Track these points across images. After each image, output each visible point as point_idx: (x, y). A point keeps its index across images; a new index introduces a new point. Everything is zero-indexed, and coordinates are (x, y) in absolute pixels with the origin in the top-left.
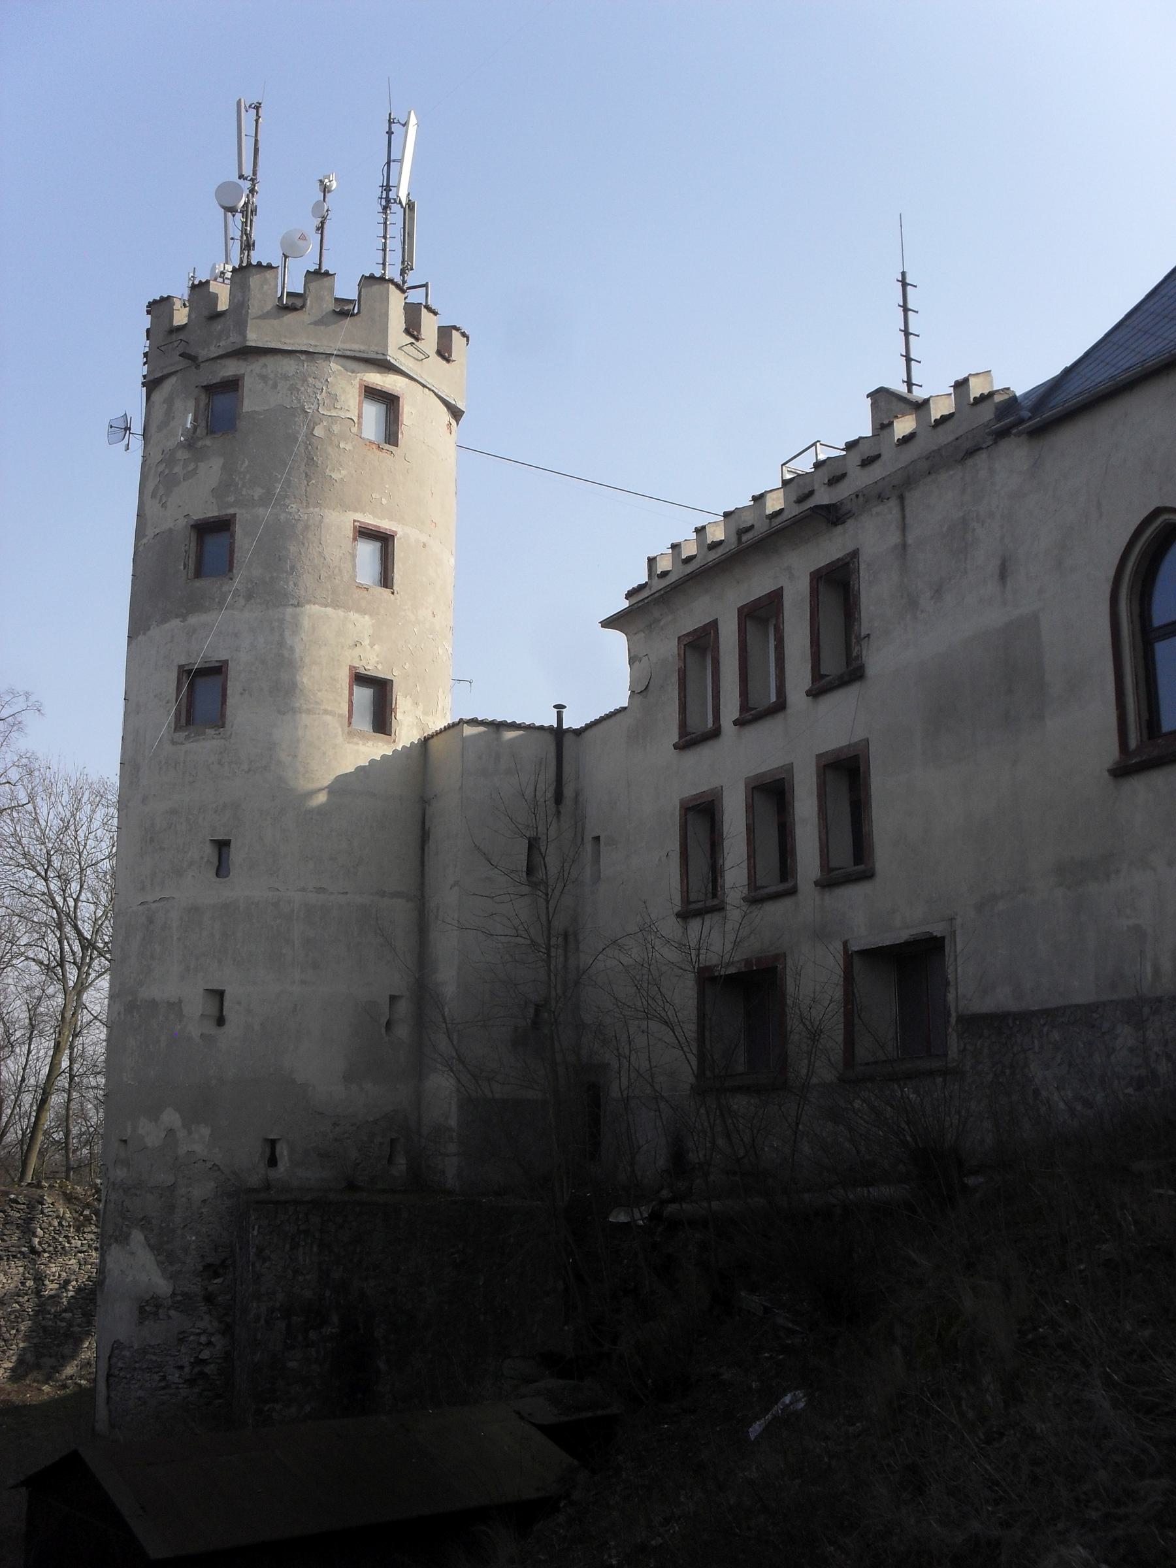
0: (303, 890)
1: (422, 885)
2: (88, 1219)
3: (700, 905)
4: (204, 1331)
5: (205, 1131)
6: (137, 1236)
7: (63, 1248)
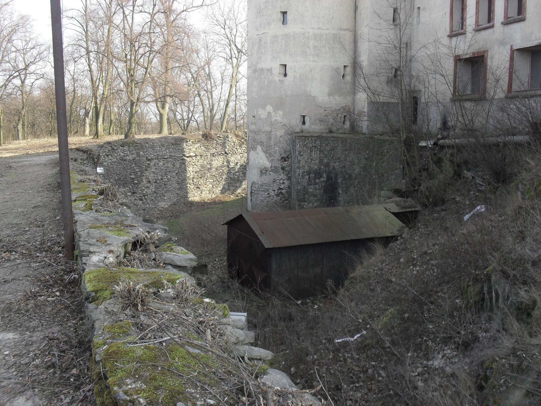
0: (313, 28)
1: (355, 26)
2: (243, 143)
3: (457, 32)
4: (282, 179)
5: (281, 113)
6: (259, 148)
7: (235, 152)
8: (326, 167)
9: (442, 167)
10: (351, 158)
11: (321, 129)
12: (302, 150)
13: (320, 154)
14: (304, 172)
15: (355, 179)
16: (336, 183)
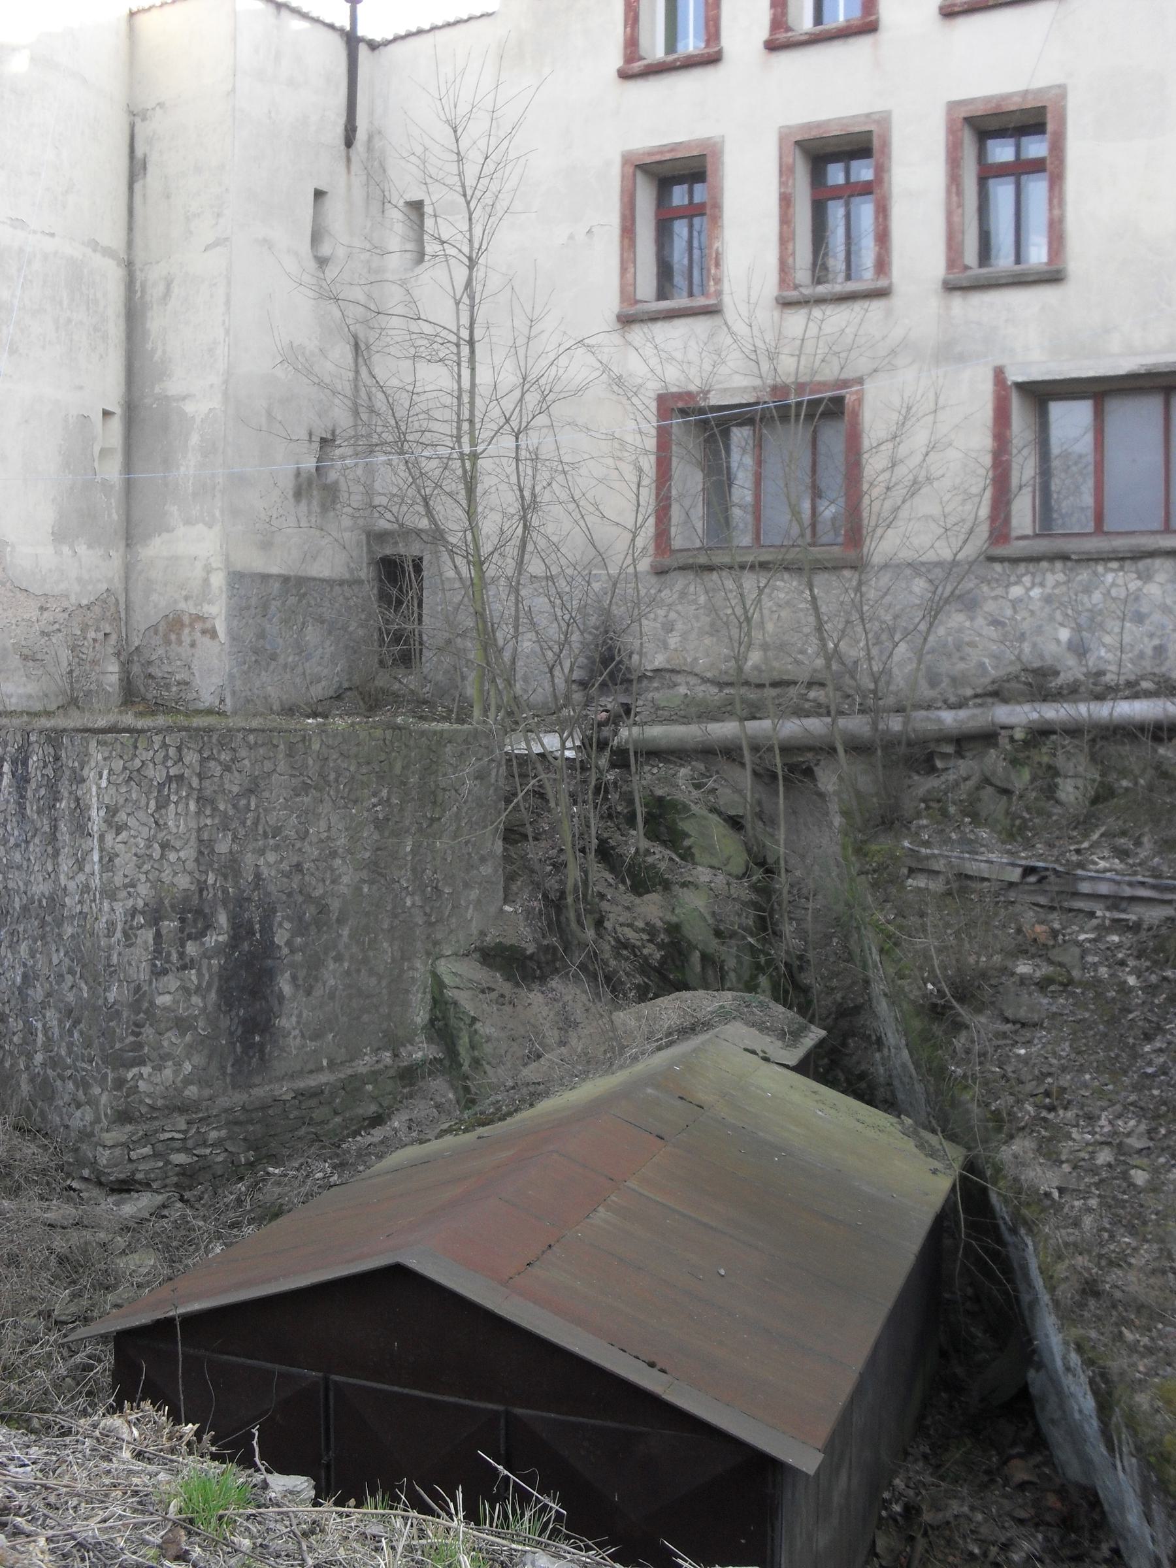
8: (225, 877)
9: (686, 835)
10: (323, 824)
11: (30, 697)
12: (121, 801)
13: (198, 813)
14: (134, 912)
15: (340, 921)
16: (269, 948)
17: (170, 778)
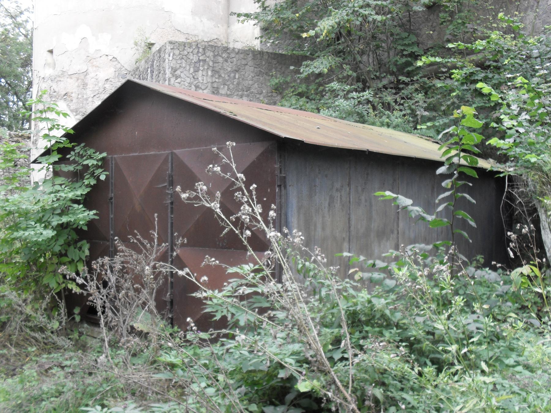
12: (178, 66)
13: (212, 76)
17: (199, 61)
